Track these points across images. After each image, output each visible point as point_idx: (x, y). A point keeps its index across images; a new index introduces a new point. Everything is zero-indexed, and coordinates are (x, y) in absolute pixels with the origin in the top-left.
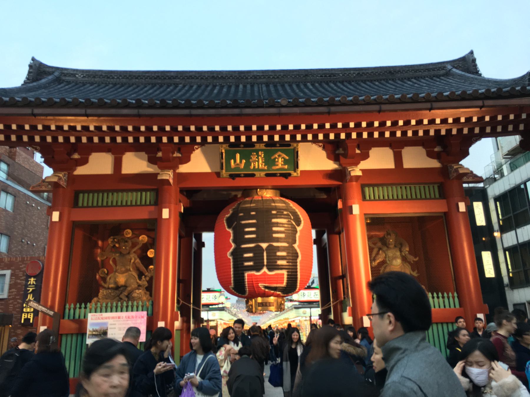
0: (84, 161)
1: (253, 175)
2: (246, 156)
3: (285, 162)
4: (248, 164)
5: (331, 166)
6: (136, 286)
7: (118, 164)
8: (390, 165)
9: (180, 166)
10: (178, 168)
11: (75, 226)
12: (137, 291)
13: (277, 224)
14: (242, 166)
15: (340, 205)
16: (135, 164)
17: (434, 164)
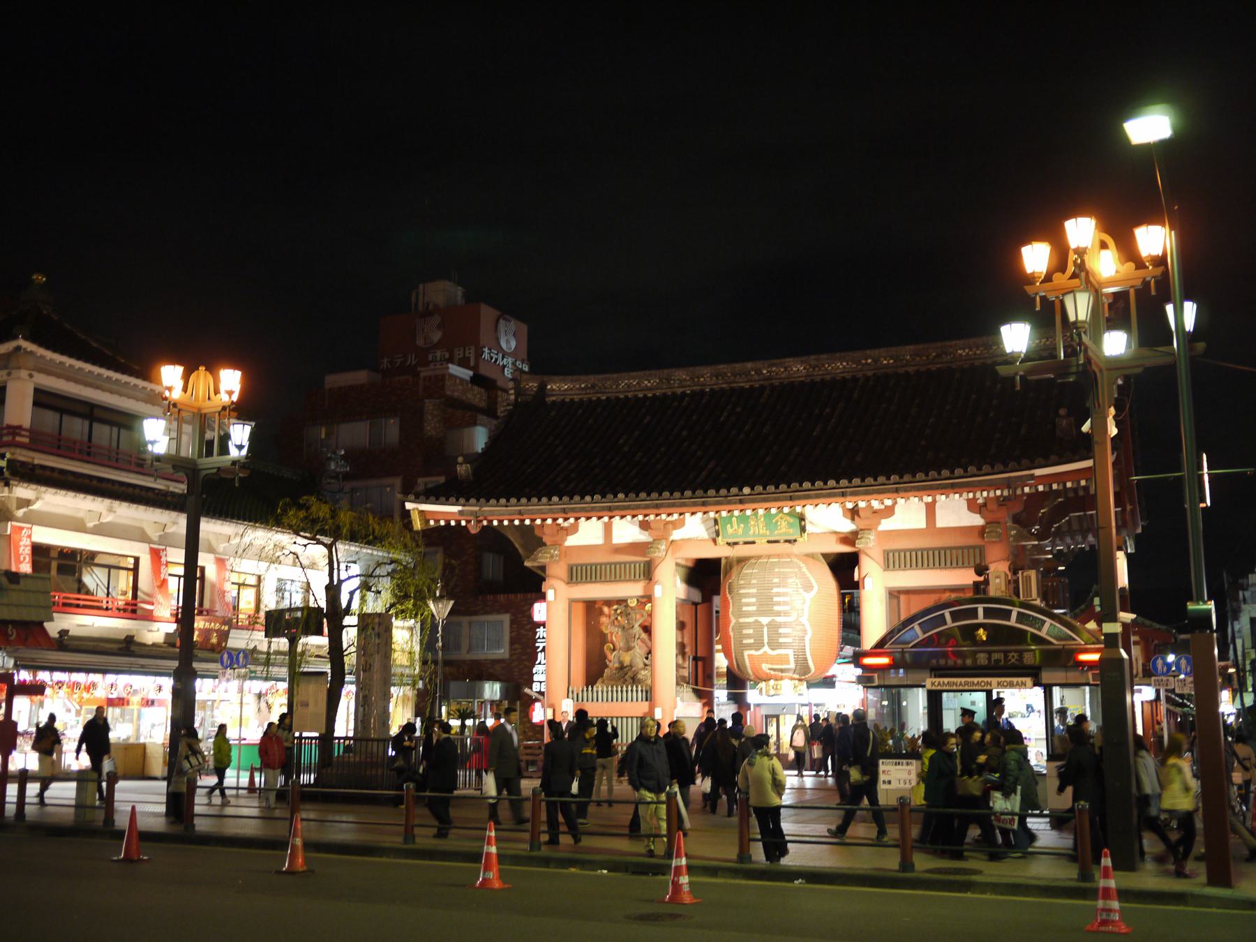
0: (574, 529)
1: (753, 543)
2: (743, 520)
3: (790, 525)
4: (746, 531)
5: (847, 526)
6: (641, 665)
7: (608, 530)
8: (919, 522)
9: (675, 532)
10: (670, 535)
11: (572, 602)
12: (643, 672)
13: (779, 604)
14: (741, 531)
15: (856, 578)
16: (626, 530)
17: (977, 520)
